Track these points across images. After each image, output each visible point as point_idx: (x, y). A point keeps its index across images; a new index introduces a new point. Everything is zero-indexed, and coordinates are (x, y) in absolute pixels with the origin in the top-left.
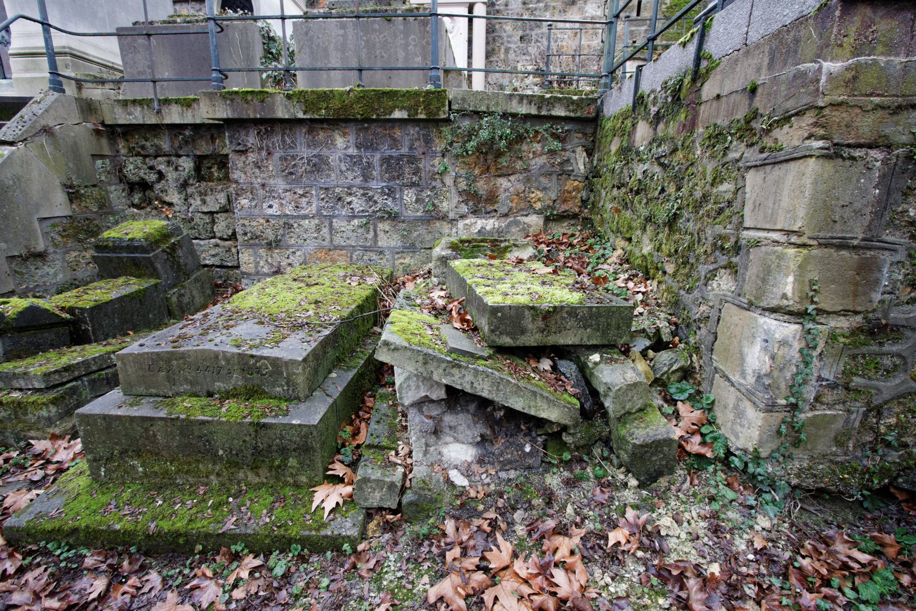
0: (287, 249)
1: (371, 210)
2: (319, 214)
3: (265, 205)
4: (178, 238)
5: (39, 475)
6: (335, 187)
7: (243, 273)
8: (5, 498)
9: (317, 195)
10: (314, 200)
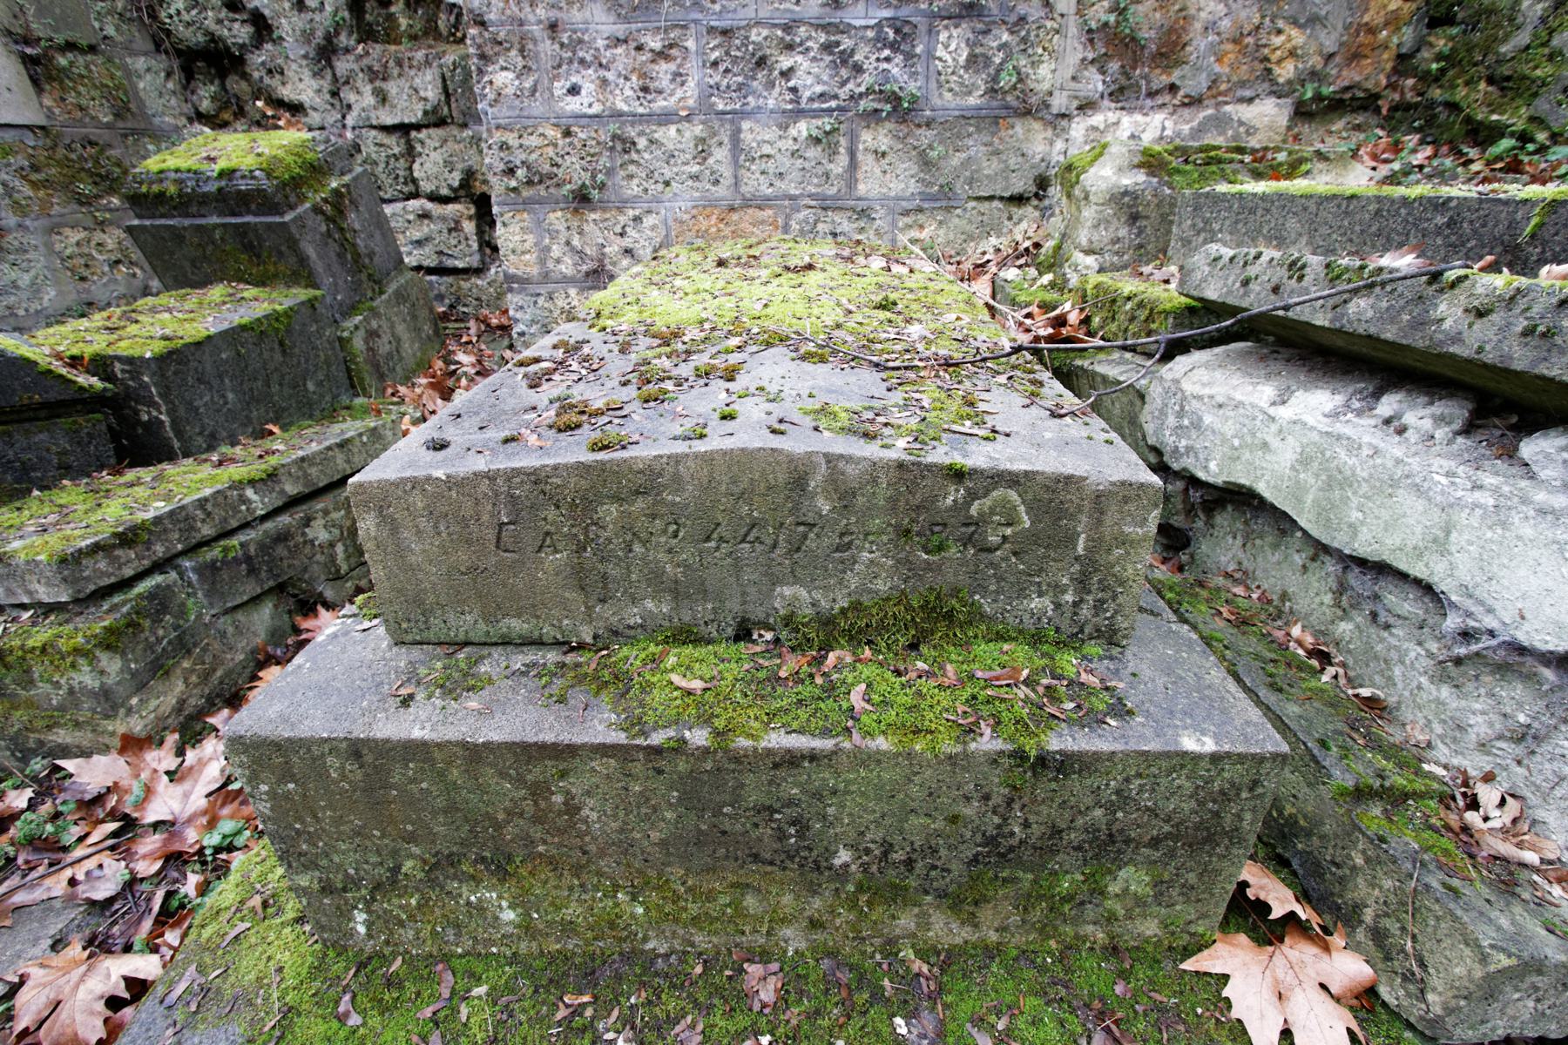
0: (620, 210)
1: (844, 93)
2: (704, 108)
3: (560, 87)
4: (347, 178)
5: (108, 878)
6: (748, 27)
7: (510, 279)
8: (14, 989)
9: (701, 53)
10: (693, 68)
